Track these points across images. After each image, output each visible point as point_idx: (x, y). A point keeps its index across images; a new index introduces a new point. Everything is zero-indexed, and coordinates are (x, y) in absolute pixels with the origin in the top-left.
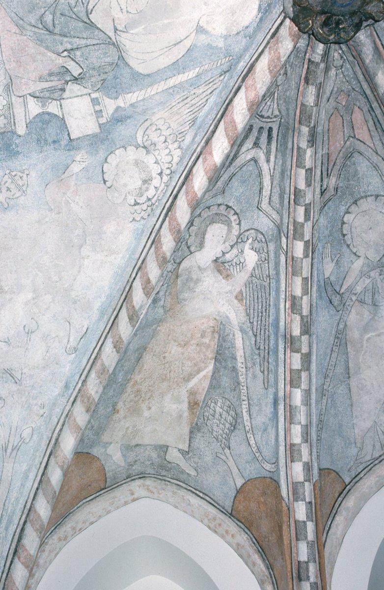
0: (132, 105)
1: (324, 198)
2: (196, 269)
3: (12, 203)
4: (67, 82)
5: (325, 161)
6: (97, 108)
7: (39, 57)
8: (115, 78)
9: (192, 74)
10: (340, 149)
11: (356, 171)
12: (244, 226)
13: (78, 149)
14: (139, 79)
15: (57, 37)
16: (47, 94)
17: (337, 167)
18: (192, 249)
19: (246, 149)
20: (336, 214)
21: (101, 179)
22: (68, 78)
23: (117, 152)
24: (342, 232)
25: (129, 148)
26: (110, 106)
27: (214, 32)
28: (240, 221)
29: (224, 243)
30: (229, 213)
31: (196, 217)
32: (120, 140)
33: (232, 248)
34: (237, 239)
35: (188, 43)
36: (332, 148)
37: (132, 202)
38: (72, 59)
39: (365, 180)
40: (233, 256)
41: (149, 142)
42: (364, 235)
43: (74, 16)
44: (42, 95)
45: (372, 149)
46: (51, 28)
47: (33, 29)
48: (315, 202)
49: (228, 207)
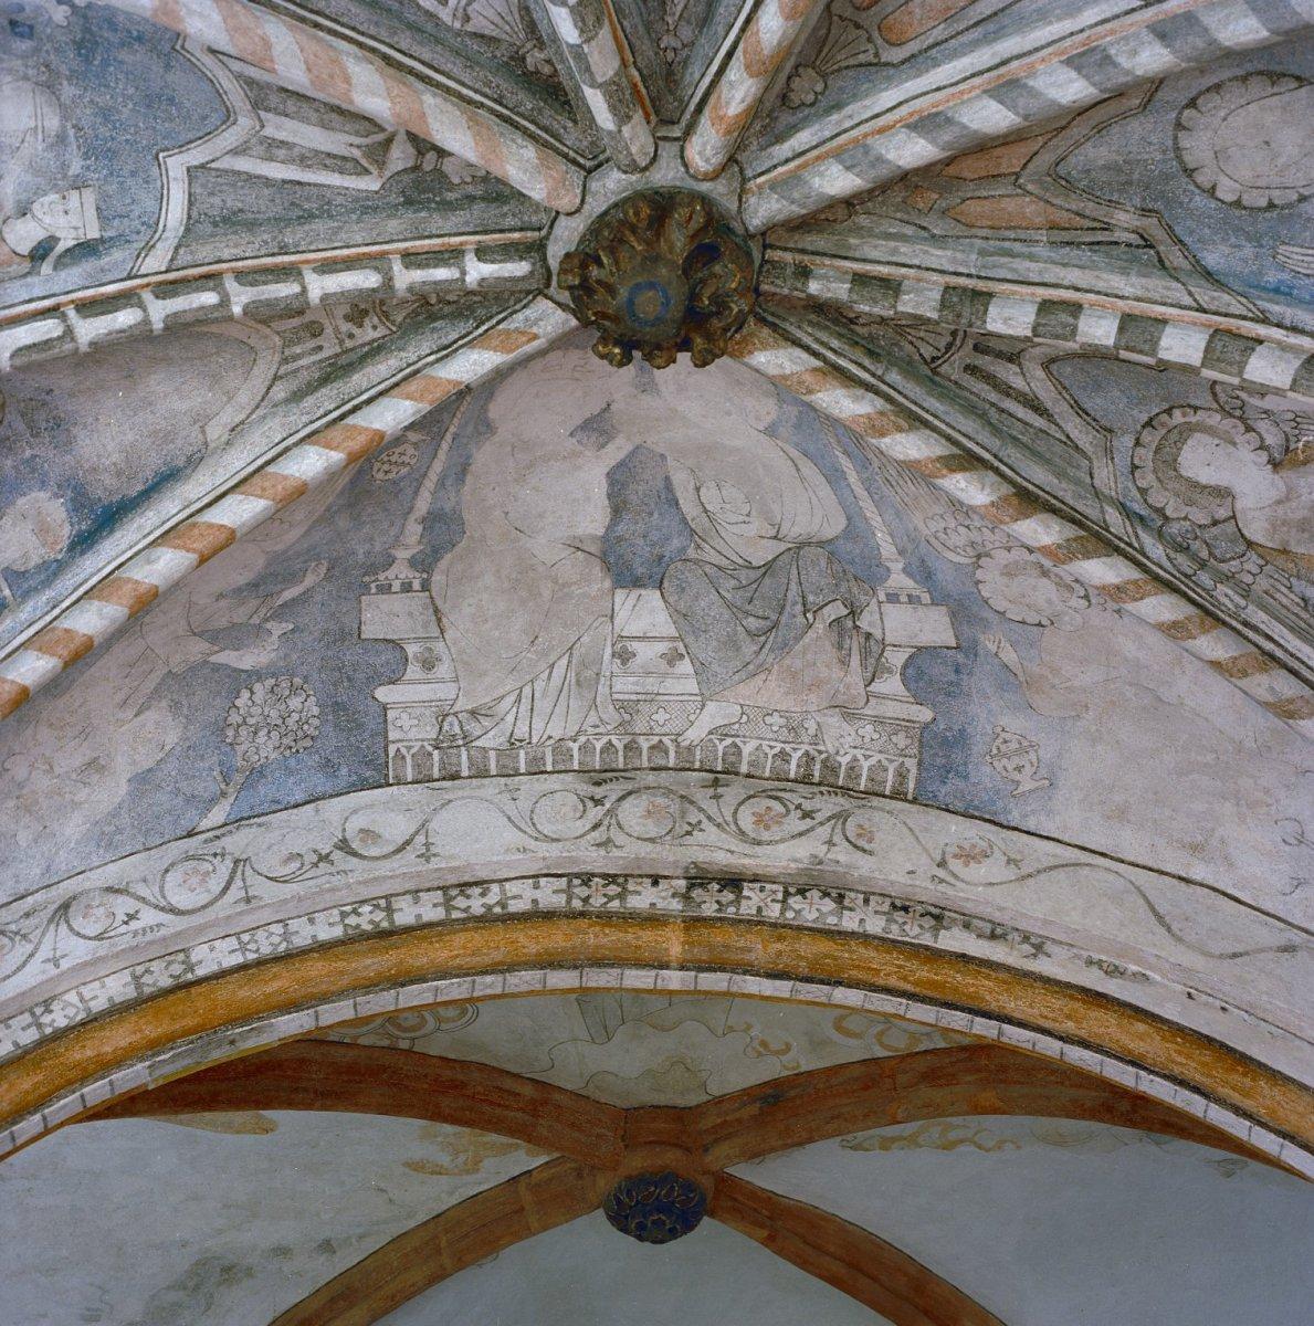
0: (901, 552)
1: (1162, 242)
2: (1280, 510)
3: (1043, 772)
4: (856, 627)
5: (1066, 236)
6: (904, 599)
7: (809, 657)
8: (852, 562)
9: (845, 463)
10: (1042, 203)
11: (1107, 168)
12: (1204, 399)
13: (975, 642)
14: (850, 533)
15: (783, 619)
16: (872, 661)
17: (1090, 208)
18: (1222, 513)
19: (1021, 377)
20: (1210, 217)
21: (1035, 628)
22: (849, 624)
23: (985, 594)
24: (1260, 209)
25: (979, 574)
26: (899, 580)
27: (774, 416)
28: (1189, 406)
29: (1234, 444)
30: (1163, 425)
31: (1145, 500)
32: (964, 584)
33: (1254, 430)
34: (1231, 416)
35: (795, 454)
36: (1038, 220)
37: (1084, 603)
38: (821, 608)
39: (1135, 149)
40: (1274, 430)
41: (968, 549)
42: (1281, 161)
43: (754, 586)
44: (870, 669)
45: (1050, 140)
46: (768, 623)
47: (765, 650)
48: (1139, 293)
49: (1149, 424)
